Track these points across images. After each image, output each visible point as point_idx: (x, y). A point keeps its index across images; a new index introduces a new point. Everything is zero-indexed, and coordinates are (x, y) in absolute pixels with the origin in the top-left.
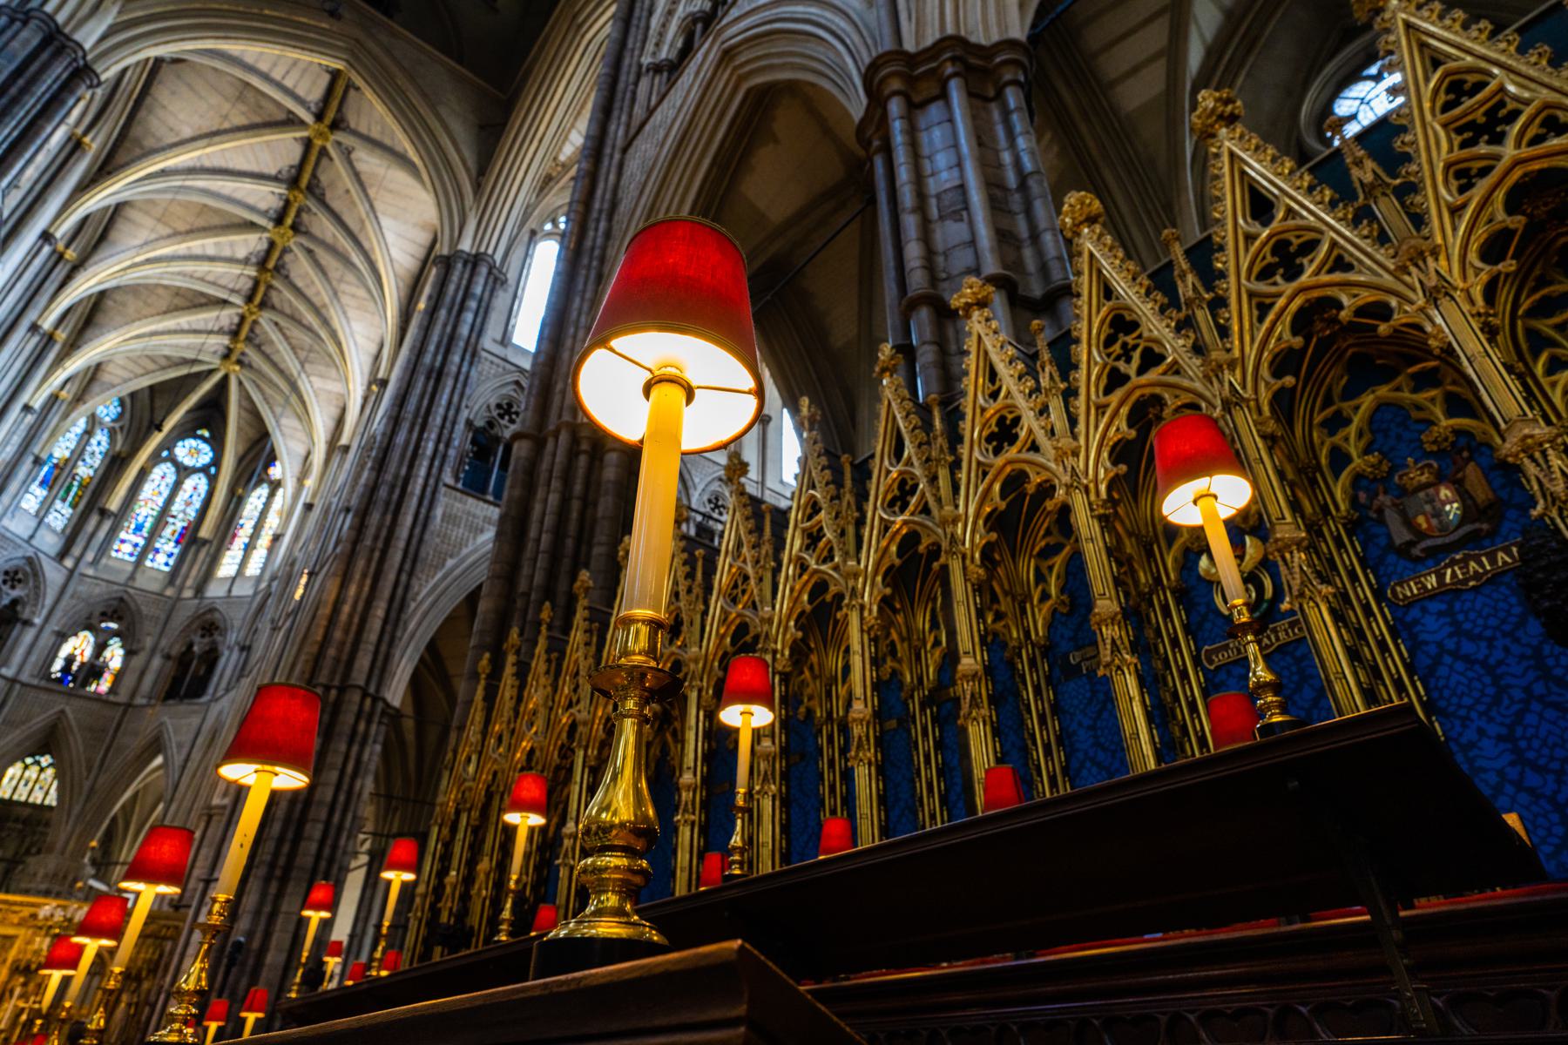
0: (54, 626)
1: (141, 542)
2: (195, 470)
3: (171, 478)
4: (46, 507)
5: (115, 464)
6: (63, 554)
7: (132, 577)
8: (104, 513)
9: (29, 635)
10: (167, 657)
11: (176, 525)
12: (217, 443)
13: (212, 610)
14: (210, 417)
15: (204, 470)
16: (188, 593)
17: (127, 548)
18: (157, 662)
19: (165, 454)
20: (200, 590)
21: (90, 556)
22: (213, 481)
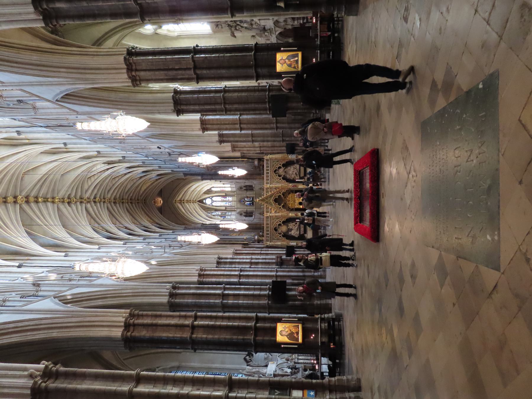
0: (246, 207)
1: (228, 202)
2: (212, 200)
3: (215, 203)
4: (228, 215)
5: (216, 210)
6: (235, 211)
7: (235, 201)
8: (226, 209)
9: (248, 209)
10: (247, 192)
11: (223, 199)
12: (205, 199)
13: (238, 189)
14: (201, 201)
15: (211, 199)
16: (236, 193)
17: (230, 204)
18: (248, 193)
19: (211, 205)
20: (234, 192)
21: (234, 207)
22: (213, 197)
